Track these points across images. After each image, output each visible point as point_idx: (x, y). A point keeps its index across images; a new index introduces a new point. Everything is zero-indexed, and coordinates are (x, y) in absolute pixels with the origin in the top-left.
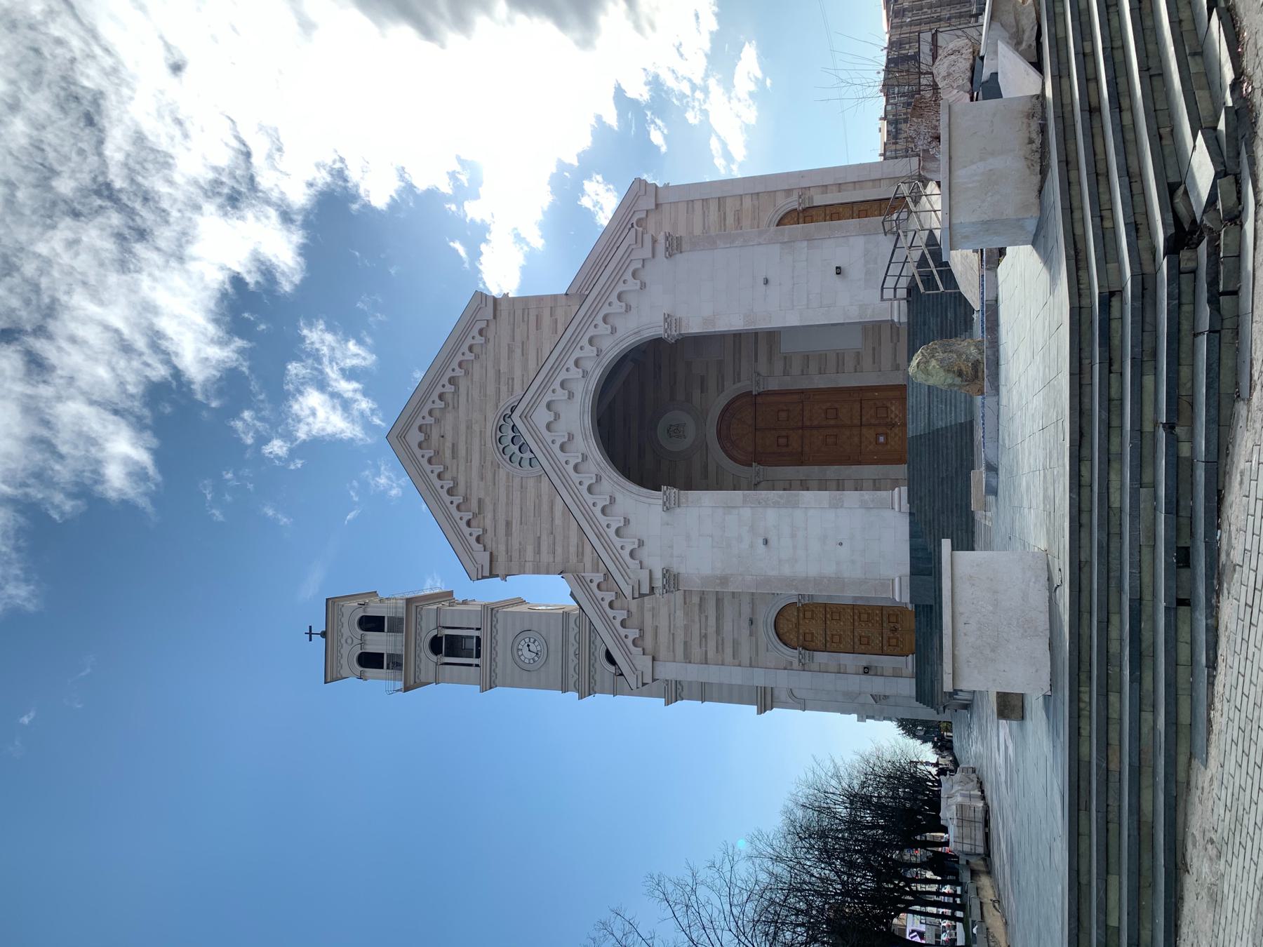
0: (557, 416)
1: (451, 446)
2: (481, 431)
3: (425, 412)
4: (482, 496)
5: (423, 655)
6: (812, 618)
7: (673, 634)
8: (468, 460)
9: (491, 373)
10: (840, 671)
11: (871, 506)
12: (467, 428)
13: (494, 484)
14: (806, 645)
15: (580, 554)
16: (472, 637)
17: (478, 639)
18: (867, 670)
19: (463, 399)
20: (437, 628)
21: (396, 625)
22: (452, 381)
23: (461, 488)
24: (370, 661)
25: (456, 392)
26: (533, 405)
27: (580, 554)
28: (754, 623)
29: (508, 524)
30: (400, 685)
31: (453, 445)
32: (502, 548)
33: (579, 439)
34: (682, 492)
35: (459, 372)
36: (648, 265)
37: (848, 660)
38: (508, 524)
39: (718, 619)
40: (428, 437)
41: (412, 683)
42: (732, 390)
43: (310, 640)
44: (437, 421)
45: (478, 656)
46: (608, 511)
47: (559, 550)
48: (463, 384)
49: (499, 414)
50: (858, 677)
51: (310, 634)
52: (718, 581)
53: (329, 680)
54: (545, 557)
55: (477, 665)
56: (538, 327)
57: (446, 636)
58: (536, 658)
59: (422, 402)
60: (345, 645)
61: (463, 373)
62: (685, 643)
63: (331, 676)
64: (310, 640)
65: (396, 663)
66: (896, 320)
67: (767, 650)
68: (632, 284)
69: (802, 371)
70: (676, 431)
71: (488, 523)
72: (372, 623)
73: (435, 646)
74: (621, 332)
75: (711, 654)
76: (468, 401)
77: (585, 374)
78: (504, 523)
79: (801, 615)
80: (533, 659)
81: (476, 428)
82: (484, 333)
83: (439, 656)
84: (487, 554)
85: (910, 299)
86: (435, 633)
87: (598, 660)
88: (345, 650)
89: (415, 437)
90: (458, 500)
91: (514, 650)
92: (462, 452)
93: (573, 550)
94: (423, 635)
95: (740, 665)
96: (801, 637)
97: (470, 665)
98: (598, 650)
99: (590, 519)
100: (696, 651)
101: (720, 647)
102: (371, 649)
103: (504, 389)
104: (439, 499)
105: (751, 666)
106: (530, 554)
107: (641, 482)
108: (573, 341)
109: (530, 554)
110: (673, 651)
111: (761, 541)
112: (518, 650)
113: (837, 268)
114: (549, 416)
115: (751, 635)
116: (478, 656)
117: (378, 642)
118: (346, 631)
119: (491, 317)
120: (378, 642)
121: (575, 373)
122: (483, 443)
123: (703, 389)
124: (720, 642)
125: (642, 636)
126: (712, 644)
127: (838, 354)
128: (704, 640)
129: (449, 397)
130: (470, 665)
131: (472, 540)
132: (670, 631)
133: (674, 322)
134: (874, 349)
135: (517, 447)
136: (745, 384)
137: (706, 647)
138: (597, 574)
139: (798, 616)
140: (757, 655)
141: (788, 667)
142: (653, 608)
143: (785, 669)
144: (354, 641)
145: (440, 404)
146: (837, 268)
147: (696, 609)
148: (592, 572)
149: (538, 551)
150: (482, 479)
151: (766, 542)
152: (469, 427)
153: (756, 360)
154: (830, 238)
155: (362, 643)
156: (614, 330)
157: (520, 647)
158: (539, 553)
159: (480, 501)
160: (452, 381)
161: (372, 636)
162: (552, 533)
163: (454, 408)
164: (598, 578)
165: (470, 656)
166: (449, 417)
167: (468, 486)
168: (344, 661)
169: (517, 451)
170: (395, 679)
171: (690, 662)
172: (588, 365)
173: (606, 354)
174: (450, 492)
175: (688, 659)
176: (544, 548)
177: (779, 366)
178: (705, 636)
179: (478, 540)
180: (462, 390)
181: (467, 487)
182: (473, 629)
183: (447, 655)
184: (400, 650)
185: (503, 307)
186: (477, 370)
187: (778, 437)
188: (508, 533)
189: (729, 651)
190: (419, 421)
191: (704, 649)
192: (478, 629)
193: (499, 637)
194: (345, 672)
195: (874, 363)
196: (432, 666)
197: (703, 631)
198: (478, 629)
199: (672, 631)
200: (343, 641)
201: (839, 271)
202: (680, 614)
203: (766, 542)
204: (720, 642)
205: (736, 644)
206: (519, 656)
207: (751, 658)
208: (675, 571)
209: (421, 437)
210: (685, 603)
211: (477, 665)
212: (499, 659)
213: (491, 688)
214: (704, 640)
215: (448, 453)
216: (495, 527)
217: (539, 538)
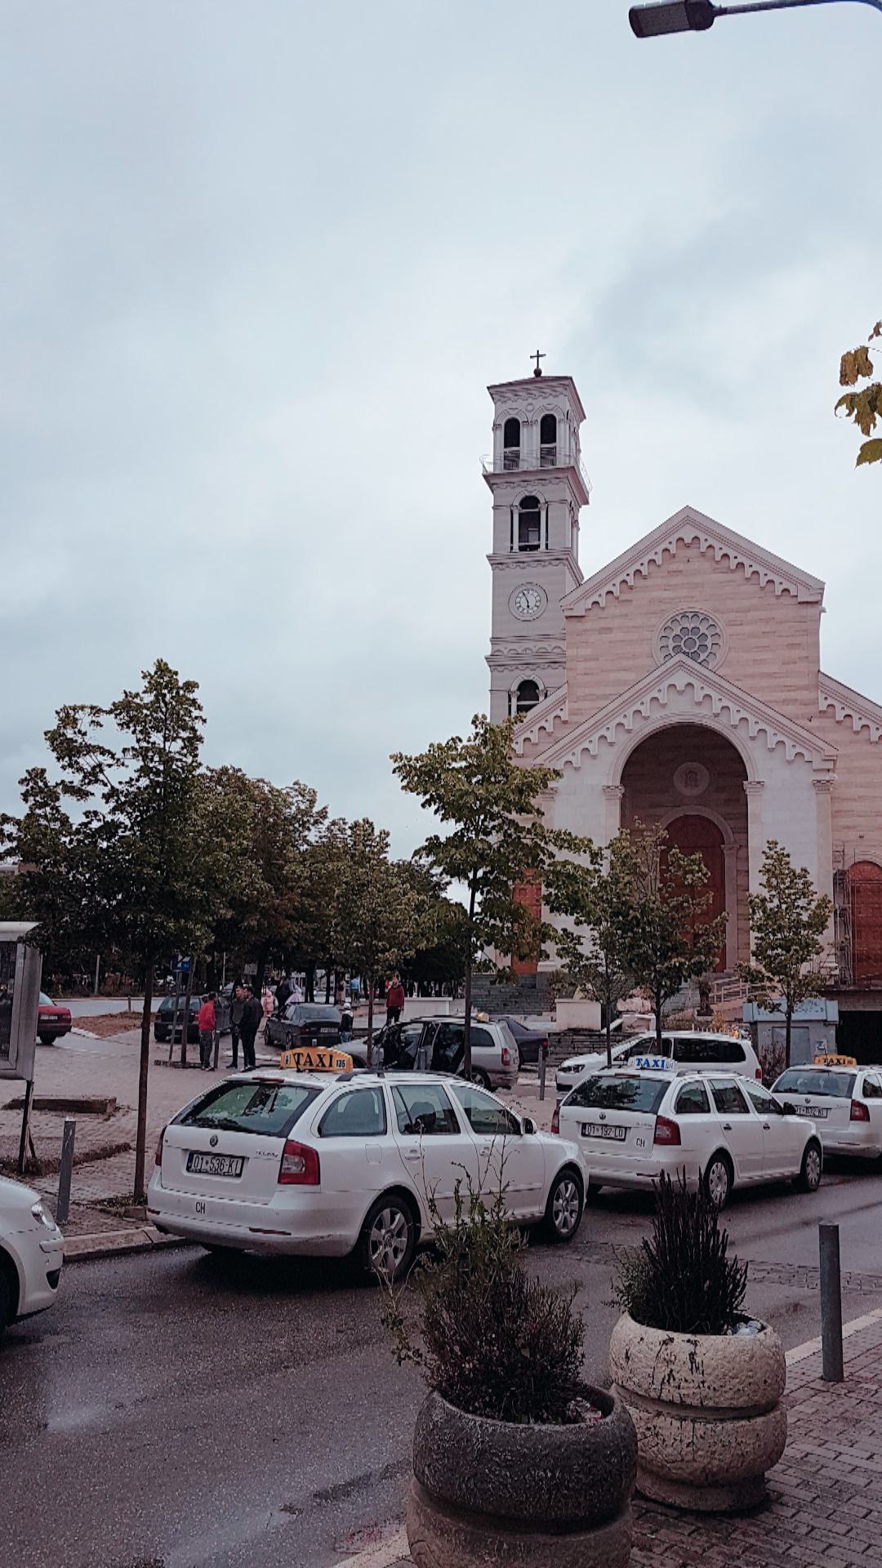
0: (681, 693)
1: (680, 569)
3: (711, 542)
4: (634, 603)
5: (519, 489)
9: (746, 603)
19: (723, 577)
21: (548, 455)
22: (741, 565)
23: (641, 583)
24: (511, 432)
25: (733, 571)
26: (691, 671)
30: (490, 469)
31: (681, 571)
33: (663, 713)
34: (618, 802)
35: (748, 572)
40: (688, 546)
41: (492, 482)
44: (703, 554)
45: (522, 549)
46: (602, 740)
48: (738, 576)
53: (491, 390)
55: (512, 548)
56: (792, 646)
57: (539, 513)
59: (721, 539)
61: (747, 576)
63: (496, 391)
68: (790, 753)
70: (691, 778)
71: (612, 611)
74: (750, 743)
77: (717, 715)
82: (786, 593)
84: (583, 614)
86: (542, 501)
88: (521, 404)
90: (631, 580)
92: (675, 580)
97: (512, 542)
99: (595, 727)
103: (732, 616)
104: (632, 561)
107: (629, 763)
108: (743, 704)
112: (528, 590)
114: (680, 686)
116: (522, 549)
117: (530, 439)
119: (800, 600)
120: (530, 439)
121: (717, 707)
123: (728, 802)
129: (725, 562)
130: (512, 542)
131: (595, 598)
135: (679, 633)
144: (530, 411)
145: (718, 555)
156: (753, 738)
157: (531, 592)
158: (585, 660)
159: (631, 601)
160: (741, 565)
161: (536, 431)
163: (715, 569)
164: (564, 716)
166: (707, 565)
172: (723, 718)
179: (596, 603)
180: (729, 577)
182: (547, 540)
183: (521, 515)
184: (524, 466)
185: (810, 611)
186: (750, 588)
190: (702, 536)
192: (547, 545)
208: (557, 798)
209: (688, 540)
211: (512, 548)
213: (492, 565)
215: (674, 567)
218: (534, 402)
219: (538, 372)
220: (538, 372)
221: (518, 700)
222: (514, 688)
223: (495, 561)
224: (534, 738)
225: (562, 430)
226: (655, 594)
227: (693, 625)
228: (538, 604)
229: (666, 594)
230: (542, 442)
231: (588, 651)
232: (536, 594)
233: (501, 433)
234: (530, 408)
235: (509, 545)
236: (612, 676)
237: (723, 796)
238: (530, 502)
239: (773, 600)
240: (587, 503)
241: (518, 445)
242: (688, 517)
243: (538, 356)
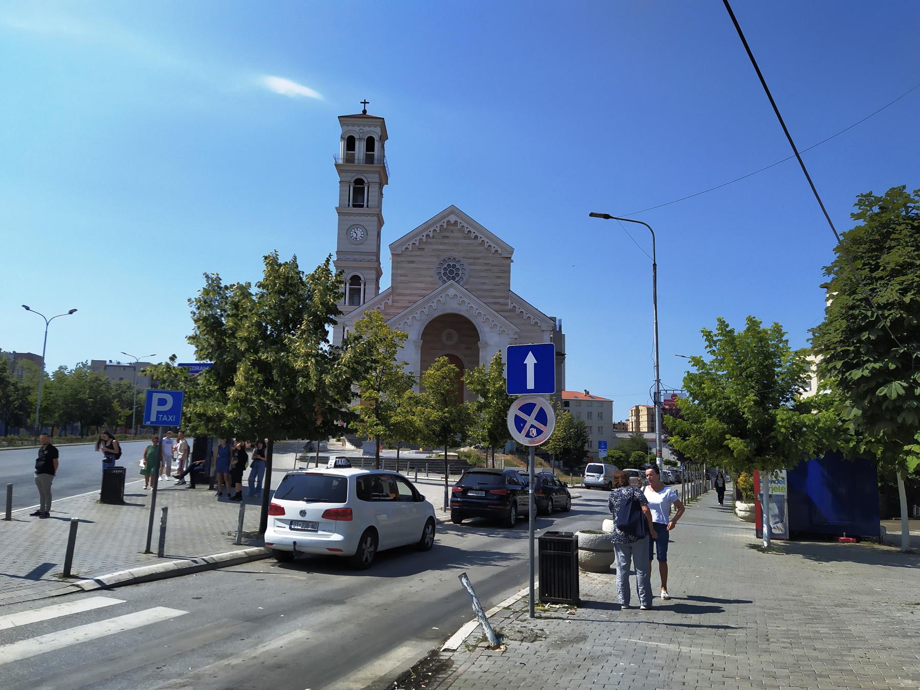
5: (354, 174)
8: (442, 244)
9: (479, 255)
12: (455, 244)
15: (400, 295)
17: (362, 206)
20: (368, 183)
21: (370, 159)
22: (476, 237)
24: (350, 143)
27: (400, 295)
30: (340, 162)
31: (448, 237)
32: (403, 259)
36: (507, 336)
38: (413, 262)
43: (361, 103)
45: (354, 206)
48: (475, 241)
51: (365, 103)
54: (399, 278)
56: (497, 277)
58: (353, 238)
60: (359, 128)
64: (361, 103)
65: (349, 159)
73: (359, 182)
78: (413, 260)
80: (353, 236)
83: (354, 184)
84: (400, 253)
86: (366, 181)
88: (357, 129)
89: (453, 219)
91: (357, 226)
92: (445, 241)
94: (365, 175)
102: (357, 143)
103: (471, 261)
106: (399, 272)
109: (399, 272)
112: (357, 228)
117: (360, 148)
118: (366, 129)
144: (360, 132)
152: (456, 244)
155: (360, 139)
158: (401, 276)
160: (476, 237)
162: (409, 282)
166: (460, 235)
167: (430, 243)
168: (350, 128)
174: (428, 236)
176: (403, 278)
180: (471, 241)
182: (368, 202)
183: (354, 188)
185: (507, 262)
190: (459, 221)
192: (368, 205)
193: (363, 218)
194: (347, 128)
196: (349, 179)
198: (368, 205)
200: (361, 127)
211: (349, 205)
212: (352, 217)
215: (445, 234)
217: (407, 276)
218: (364, 128)
219: (365, 111)
220: (365, 111)
221: (350, 285)
223: (340, 212)
226: (436, 247)
227: (453, 263)
228: (362, 236)
229: (441, 247)
230: (367, 151)
231: (403, 272)
232: (361, 231)
234: (361, 131)
235: (348, 203)
236: (413, 285)
238: (359, 182)
239: (490, 255)
241: (354, 151)
243: (365, 103)
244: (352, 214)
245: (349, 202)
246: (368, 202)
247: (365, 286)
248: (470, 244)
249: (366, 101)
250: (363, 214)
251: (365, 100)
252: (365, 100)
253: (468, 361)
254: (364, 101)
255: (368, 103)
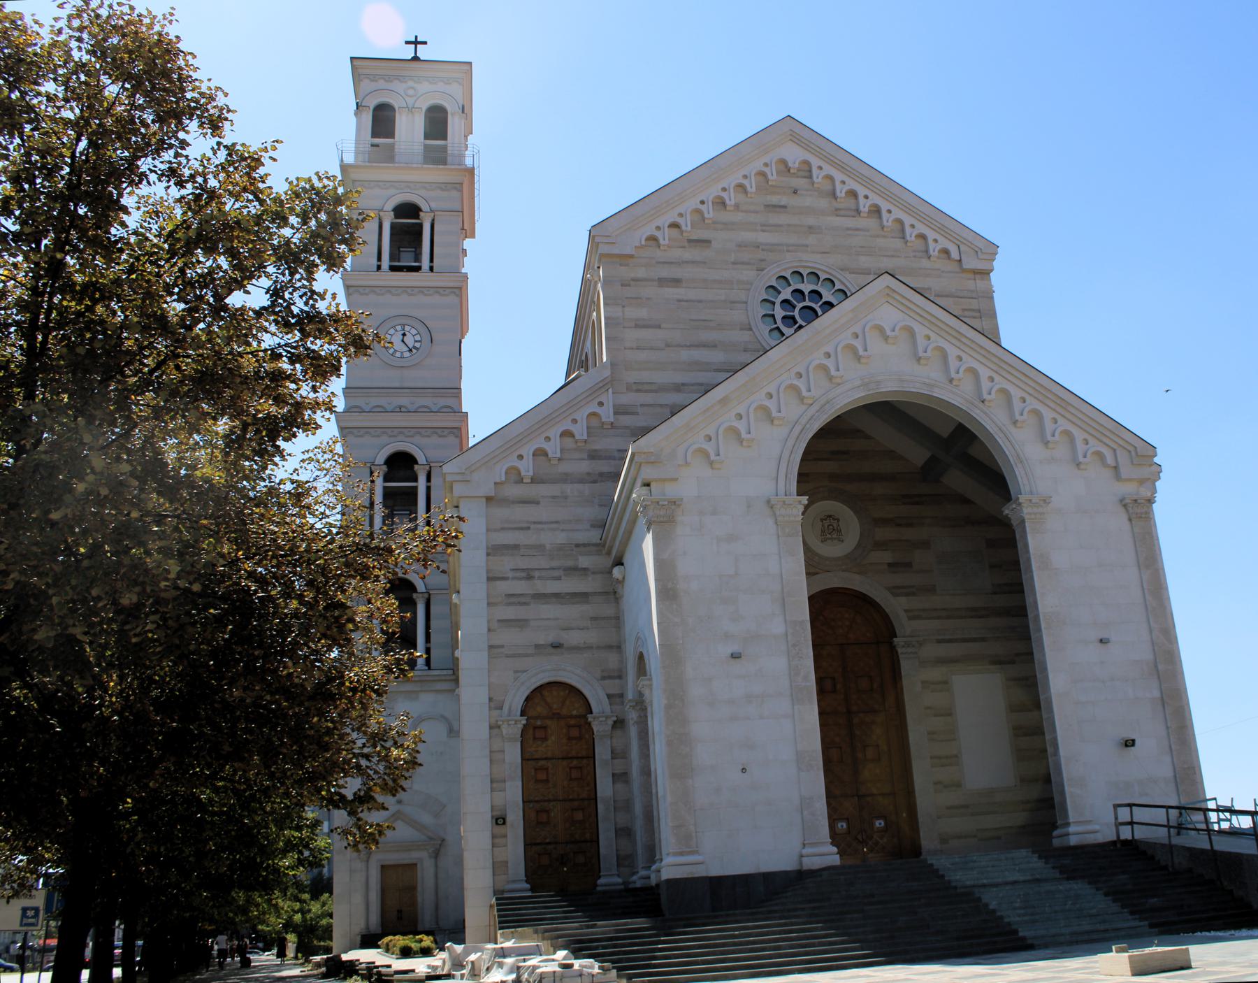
1: (783, 203)
2: (807, 246)
6: (570, 739)
7: (529, 528)
8: (765, 227)
10: (496, 783)
11: (805, 813)
12: (810, 227)
13: (734, 263)
14: (532, 733)
16: (418, 257)
17: (418, 269)
18: (500, 820)
28: (553, 650)
29: (676, 282)
31: (784, 207)
32: (641, 273)
37: (514, 792)
38: (676, 282)
39: (557, 596)
42: (896, 606)
43: (407, 43)
45: (393, 269)
47: (643, 356)
49: (834, 273)
50: (488, 808)
51: (416, 43)
52: (670, 585)
54: (632, 336)
55: (379, 268)
57: (420, 226)
59: (841, 167)
62: (516, 547)
64: (407, 43)
66: (1072, 829)
67: (516, 672)
69: (929, 708)
72: (437, 122)
75: (504, 587)
76: (848, 229)
79: (572, 722)
81: (811, 240)
84: (628, 251)
85: (1119, 845)
87: (393, 439)
89: (794, 155)
92: (775, 219)
93: (645, 376)
95: (489, 630)
96: (539, 723)
97: (379, 259)
98: (406, 439)
100: (506, 564)
101: (513, 599)
105: (491, 647)
106: (633, 313)
109: (633, 313)
110: (503, 529)
111: (735, 648)
113: (1133, 741)
115: (537, 646)
122: (790, 248)
124: (523, 600)
125: (520, 480)
126: (520, 587)
127: (956, 756)
128: (524, 574)
132: (535, 523)
133: (1040, 510)
134: (966, 807)
136: (905, 627)
137: (514, 578)
138: (612, 414)
139: (572, 717)
140: (508, 656)
141: (495, 704)
142: (566, 498)
143: (490, 699)
146: (1133, 741)
147: (570, 563)
148: (614, 406)
149: (639, 325)
150: (740, 246)
151: (735, 656)
152: (811, 229)
153: (939, 641)
154: (1167, 728)
155: (411, 110)
158: (637, 326)
159: (708, 242)
161: (419, 123)
162: (668, 345)
165: (392, 258)
166: (824, 203)
167: (727, 226)
169: (782, 297)
170: (357, 153)
171: (488, 554)
173: (985, 413)
175: (494, 551)
177: (934, 674)
178: (529, 578)
181: (725, 224)
182: (432, 260)
183: (393, 226)
187: (833, 679)
188: (662, 282)
189: (510, 613)
190: (815, 162)
191: (510, 575)
192: (431, 269)
195: (949, 808)
197: (537, 574)
198: (431, 269)
199: (532, 526)
200: (411, 83)
201: (1129, 743)
202: (561, 538)
203: (735, 656)
204: (523, 600)
205: (521, 623)
206: (394, 327)
207: (502, 646)
209: (794, 164)
210: (577, 546)
211: (379, 268)
214: (524, 574)
216: (672, 263)
217: (659, 327)
221: (386, 479)
222: (381, 459)
224: (553, 449)
225: (454, 124)
229: (764, 238)
231: (643, 313)
232: (414, 332)
233: (368, 118)
234: (411, 92)
235: (374, 261)
237: (886, 557)
240: (473, 236)
242: (791, 129)
244: (389, 289)
245: (379, 259)
246: (432, 260)
247: (429, 479)
248: (857, 229)
249: (419, 40)
250: (422, 290)
251: (416, 37)
252: (416, 37)
253: (906, 611)
254: (414, 40)
255: (425, 43)
